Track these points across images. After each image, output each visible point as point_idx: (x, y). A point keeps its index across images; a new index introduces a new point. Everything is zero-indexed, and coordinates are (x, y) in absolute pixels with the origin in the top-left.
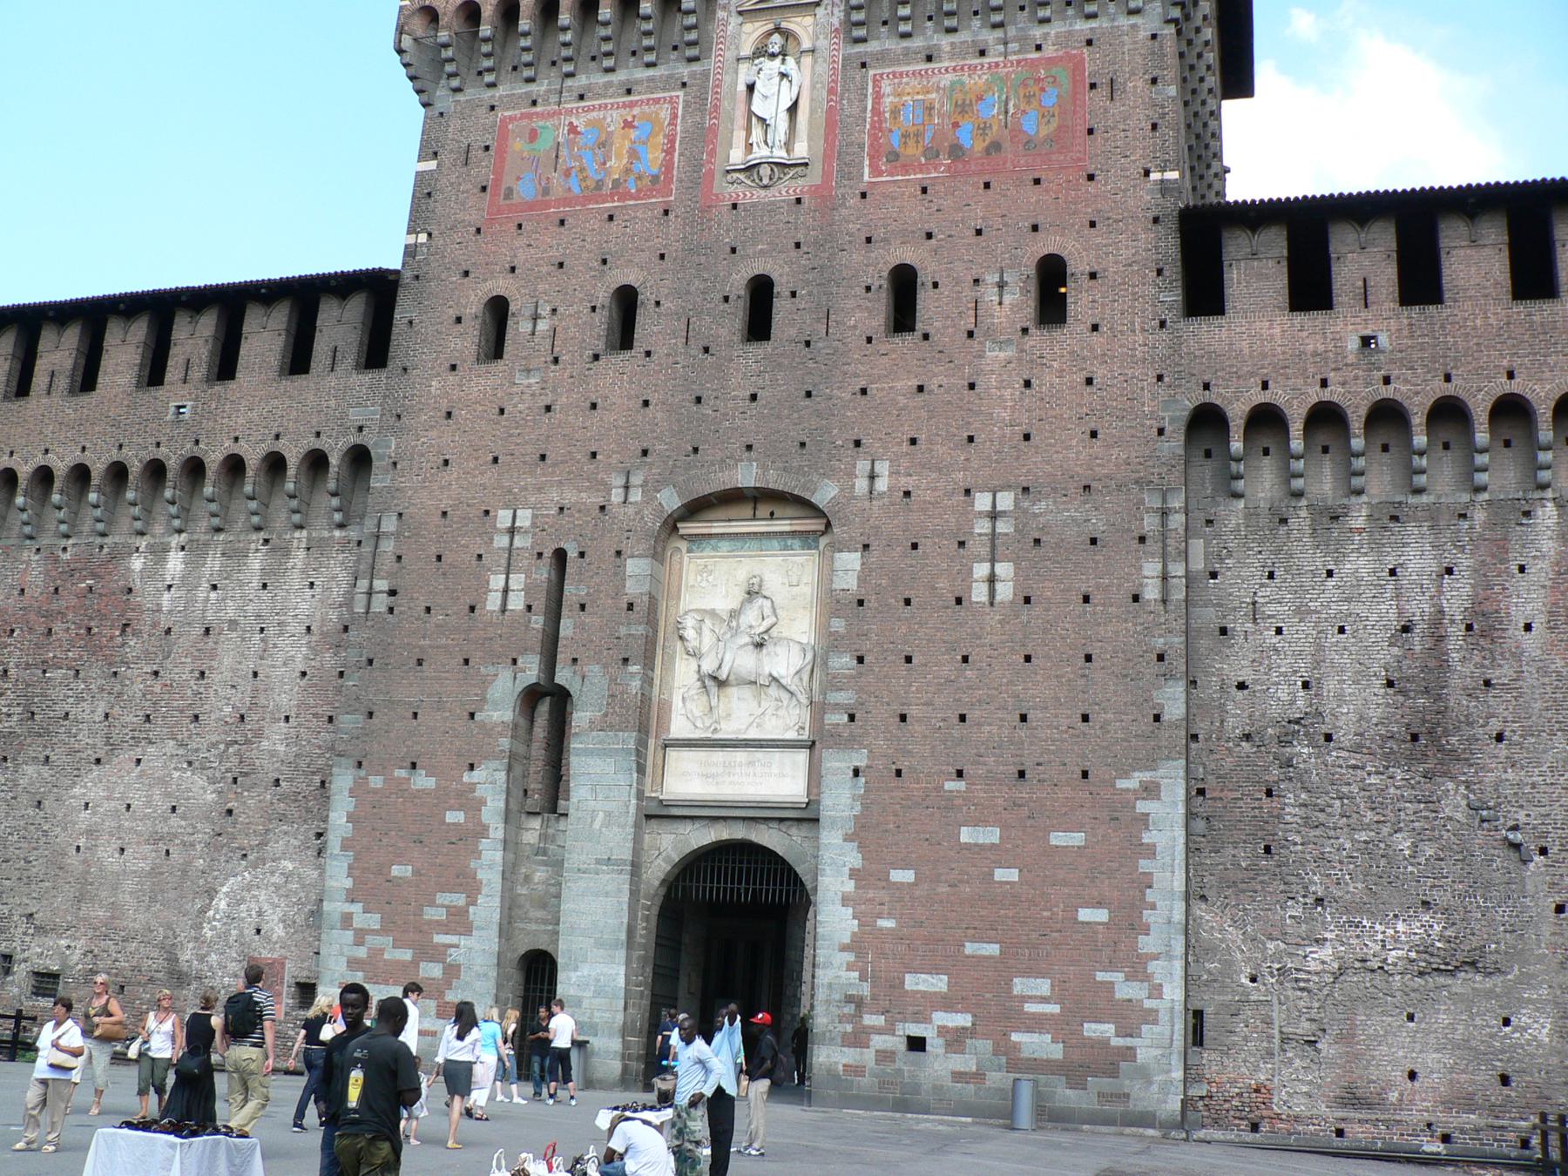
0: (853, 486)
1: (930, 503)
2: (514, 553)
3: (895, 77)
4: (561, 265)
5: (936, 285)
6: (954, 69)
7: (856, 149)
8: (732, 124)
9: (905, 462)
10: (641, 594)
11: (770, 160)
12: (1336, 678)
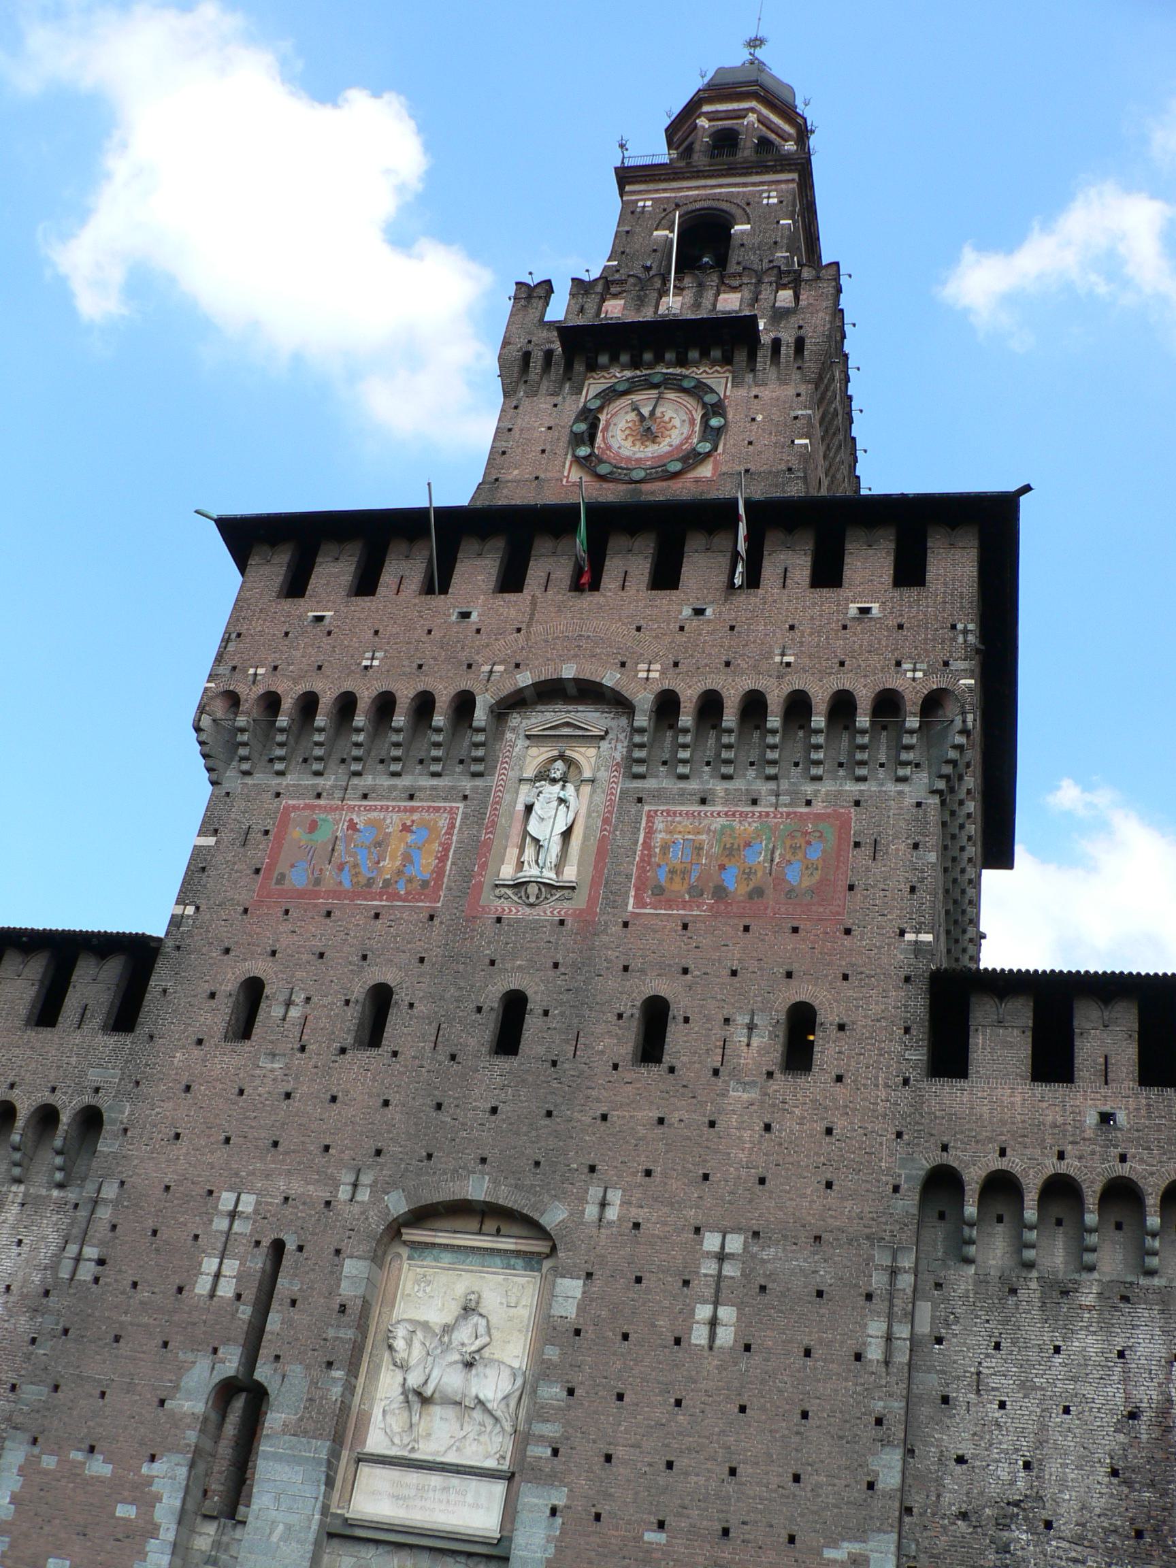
0: (583, 1212)
2: (232, 1237)
3: (668, 815)
4: (321, 955)
5: (686, 1020)
7: (622, 879)
8: (507, 841)
9: (638, 1194)
10: (356, 1296)
11: (539, 880)
12: (1059, 1461)
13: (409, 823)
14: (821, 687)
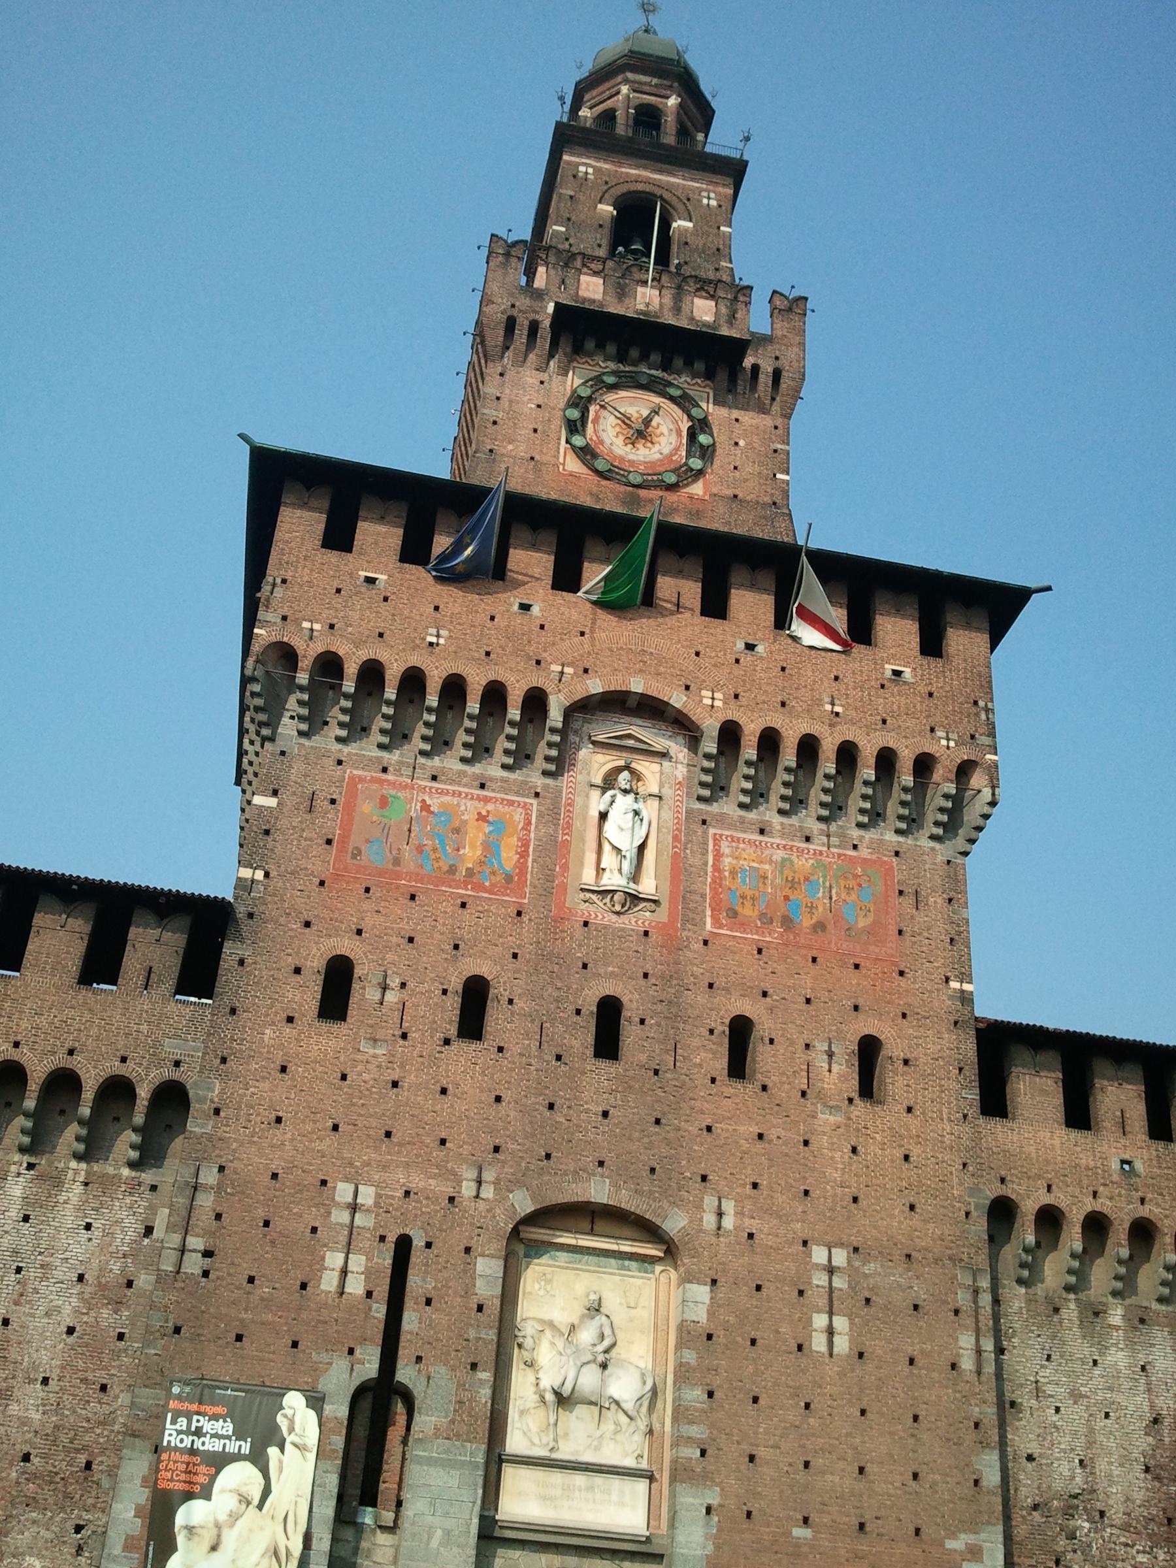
0: (701, 1220)
1: (771, 1247)
4: (411, 940)
5: (772, 1041)
6: (784, 847)
7: (698, 898)
10: (493, 1296)
12: (1106, 1459)
13: (484, 813)
14: (869, 742)
